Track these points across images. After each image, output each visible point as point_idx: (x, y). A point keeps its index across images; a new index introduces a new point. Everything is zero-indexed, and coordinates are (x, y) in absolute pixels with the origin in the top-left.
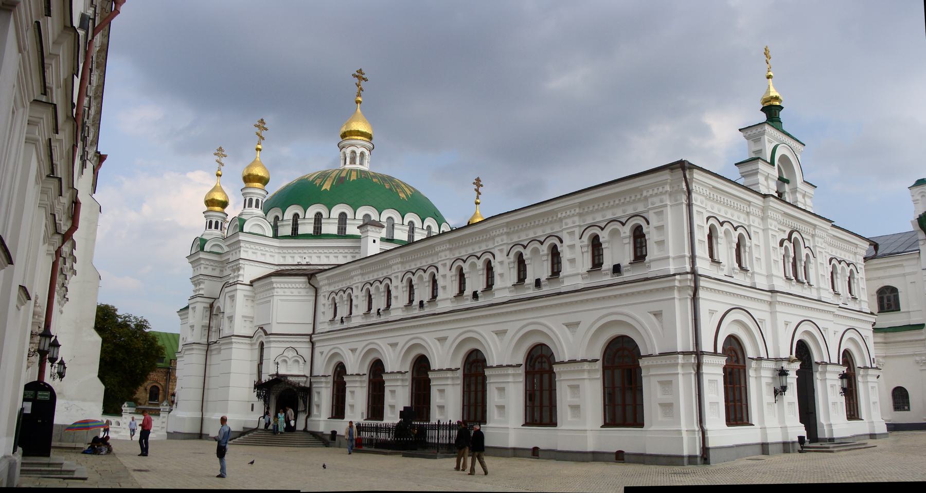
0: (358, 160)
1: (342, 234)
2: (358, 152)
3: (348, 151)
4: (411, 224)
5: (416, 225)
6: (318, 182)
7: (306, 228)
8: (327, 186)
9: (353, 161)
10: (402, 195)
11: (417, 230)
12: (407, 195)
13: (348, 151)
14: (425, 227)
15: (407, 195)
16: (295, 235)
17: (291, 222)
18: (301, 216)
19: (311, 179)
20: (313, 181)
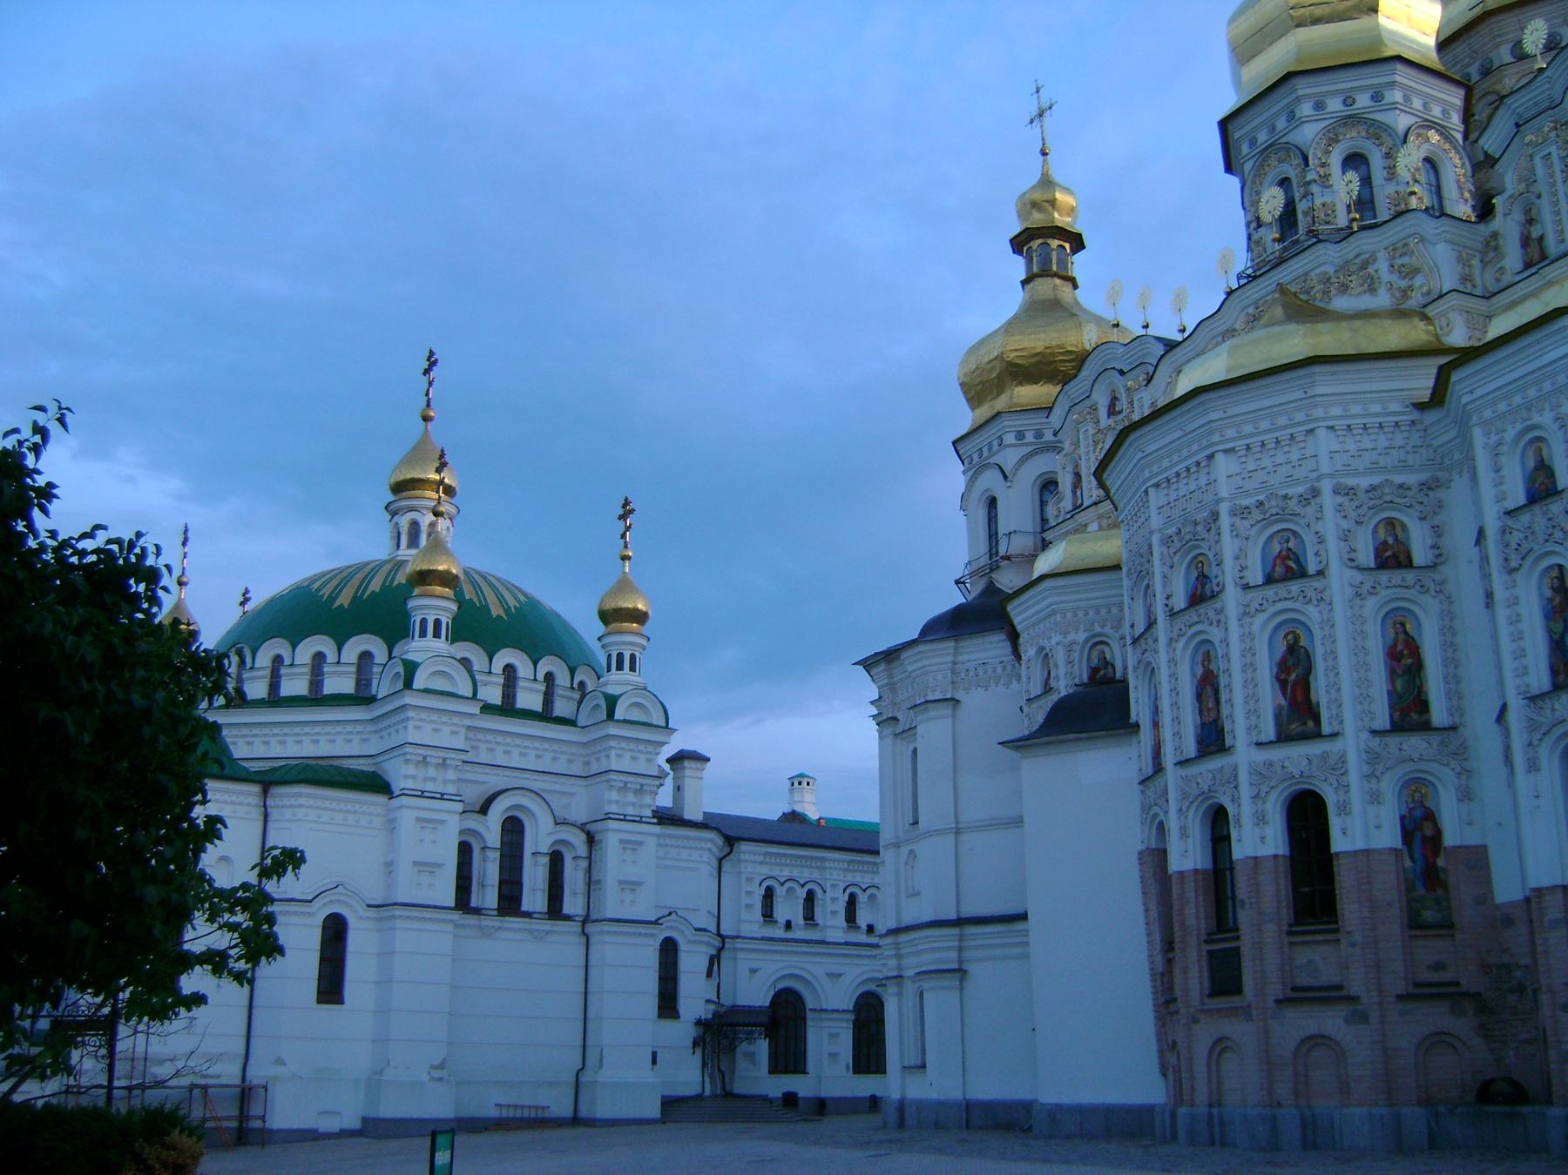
1: (362, 697)
3: (404, 521)
4: (509, 670)
6: (326, 592)
7: (296, 685)
8: (344, 599)
9: (414, 541)
10: (496, 611)
11: (521, 683)
12: (507, 611)
13: (404, 521)
14: (541, 677)
15: (507, 611)
16: (275, 700)
17: (267, 673)
18: (287, 661)
19: (315, 586)
20: (318, 590)
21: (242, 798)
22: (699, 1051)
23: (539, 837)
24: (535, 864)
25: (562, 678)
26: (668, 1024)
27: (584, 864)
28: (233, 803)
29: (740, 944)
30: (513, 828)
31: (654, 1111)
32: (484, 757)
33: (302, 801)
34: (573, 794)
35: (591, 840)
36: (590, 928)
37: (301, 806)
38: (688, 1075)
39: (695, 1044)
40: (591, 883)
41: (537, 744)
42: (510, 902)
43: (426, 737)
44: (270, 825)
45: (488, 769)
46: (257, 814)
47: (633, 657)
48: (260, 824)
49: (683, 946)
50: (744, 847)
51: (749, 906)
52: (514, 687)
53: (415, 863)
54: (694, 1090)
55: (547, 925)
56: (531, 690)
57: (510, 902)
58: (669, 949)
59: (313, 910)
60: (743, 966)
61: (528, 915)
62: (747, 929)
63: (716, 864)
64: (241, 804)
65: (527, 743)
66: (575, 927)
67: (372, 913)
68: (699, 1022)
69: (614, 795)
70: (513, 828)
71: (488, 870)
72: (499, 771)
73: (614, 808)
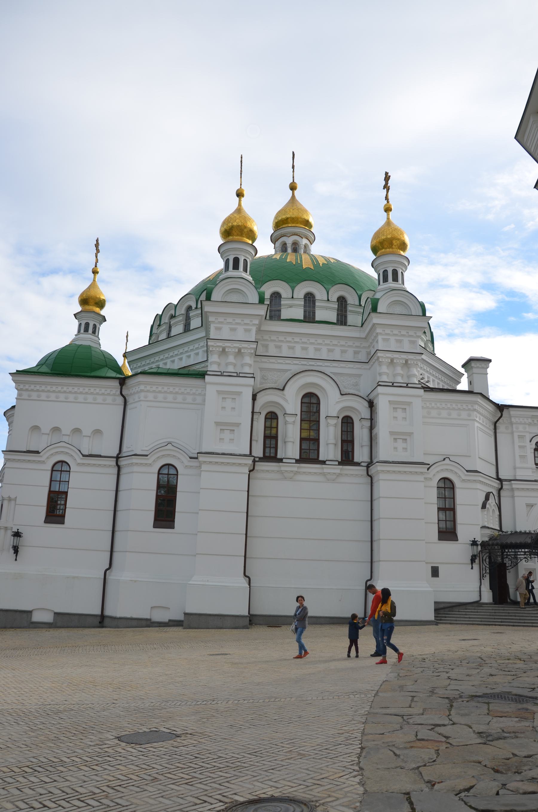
0: (289, 250)
2: (289, 241)
5: (318, 297)
11: (317, 304)
14: (334, 297)
21: (108, 391)
22: (476, 566)
23: (331, 406)
24: (328, 425)
25: (352, 299)
26: (448, 546)
27: (368, 424)
28: (103, 394)
29: (515, 485)
30: (311, 403)
31: (430, 616)
32: (285, 352)
33: (142, 387)
34: (359, 376)
35: (371, 404)
36: (373, 470)
37: (142, 391)
38: (467, 584)
39: (473, 560)
40: (372, 439)
41: (327, 341)
42: (309, 454)
43: (225, 334)
44: (129, 407)
45: (288, 361)
46: (120, 400)
47: (395, 273)
48: (122, 407)
49: (458, 484)
50: (513, 412)
51: (522, 457)
52: (314, 306)
53: (217, 424)
54: (473, 597)
55: (338, 469)
56: (327, 308)
57: (309, 454)
58: (447, 487)
59: (150, 461)
60: (521, 502)
61: (323, 462)
62: (520, 474)
63: (493, 427)
64: (109, 394)
65: (320, 341)
66: (361, 470)
67: (194, 463)
68: (474, 543)
69: (384, 369)
70: (311, 403)
71: (291, 434)
72: (296, 361)
73: (385, 378)
